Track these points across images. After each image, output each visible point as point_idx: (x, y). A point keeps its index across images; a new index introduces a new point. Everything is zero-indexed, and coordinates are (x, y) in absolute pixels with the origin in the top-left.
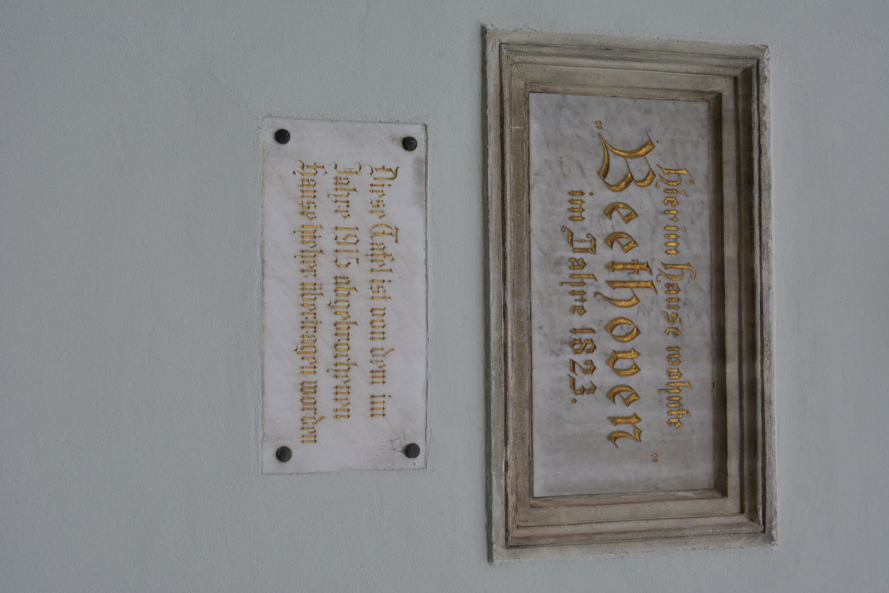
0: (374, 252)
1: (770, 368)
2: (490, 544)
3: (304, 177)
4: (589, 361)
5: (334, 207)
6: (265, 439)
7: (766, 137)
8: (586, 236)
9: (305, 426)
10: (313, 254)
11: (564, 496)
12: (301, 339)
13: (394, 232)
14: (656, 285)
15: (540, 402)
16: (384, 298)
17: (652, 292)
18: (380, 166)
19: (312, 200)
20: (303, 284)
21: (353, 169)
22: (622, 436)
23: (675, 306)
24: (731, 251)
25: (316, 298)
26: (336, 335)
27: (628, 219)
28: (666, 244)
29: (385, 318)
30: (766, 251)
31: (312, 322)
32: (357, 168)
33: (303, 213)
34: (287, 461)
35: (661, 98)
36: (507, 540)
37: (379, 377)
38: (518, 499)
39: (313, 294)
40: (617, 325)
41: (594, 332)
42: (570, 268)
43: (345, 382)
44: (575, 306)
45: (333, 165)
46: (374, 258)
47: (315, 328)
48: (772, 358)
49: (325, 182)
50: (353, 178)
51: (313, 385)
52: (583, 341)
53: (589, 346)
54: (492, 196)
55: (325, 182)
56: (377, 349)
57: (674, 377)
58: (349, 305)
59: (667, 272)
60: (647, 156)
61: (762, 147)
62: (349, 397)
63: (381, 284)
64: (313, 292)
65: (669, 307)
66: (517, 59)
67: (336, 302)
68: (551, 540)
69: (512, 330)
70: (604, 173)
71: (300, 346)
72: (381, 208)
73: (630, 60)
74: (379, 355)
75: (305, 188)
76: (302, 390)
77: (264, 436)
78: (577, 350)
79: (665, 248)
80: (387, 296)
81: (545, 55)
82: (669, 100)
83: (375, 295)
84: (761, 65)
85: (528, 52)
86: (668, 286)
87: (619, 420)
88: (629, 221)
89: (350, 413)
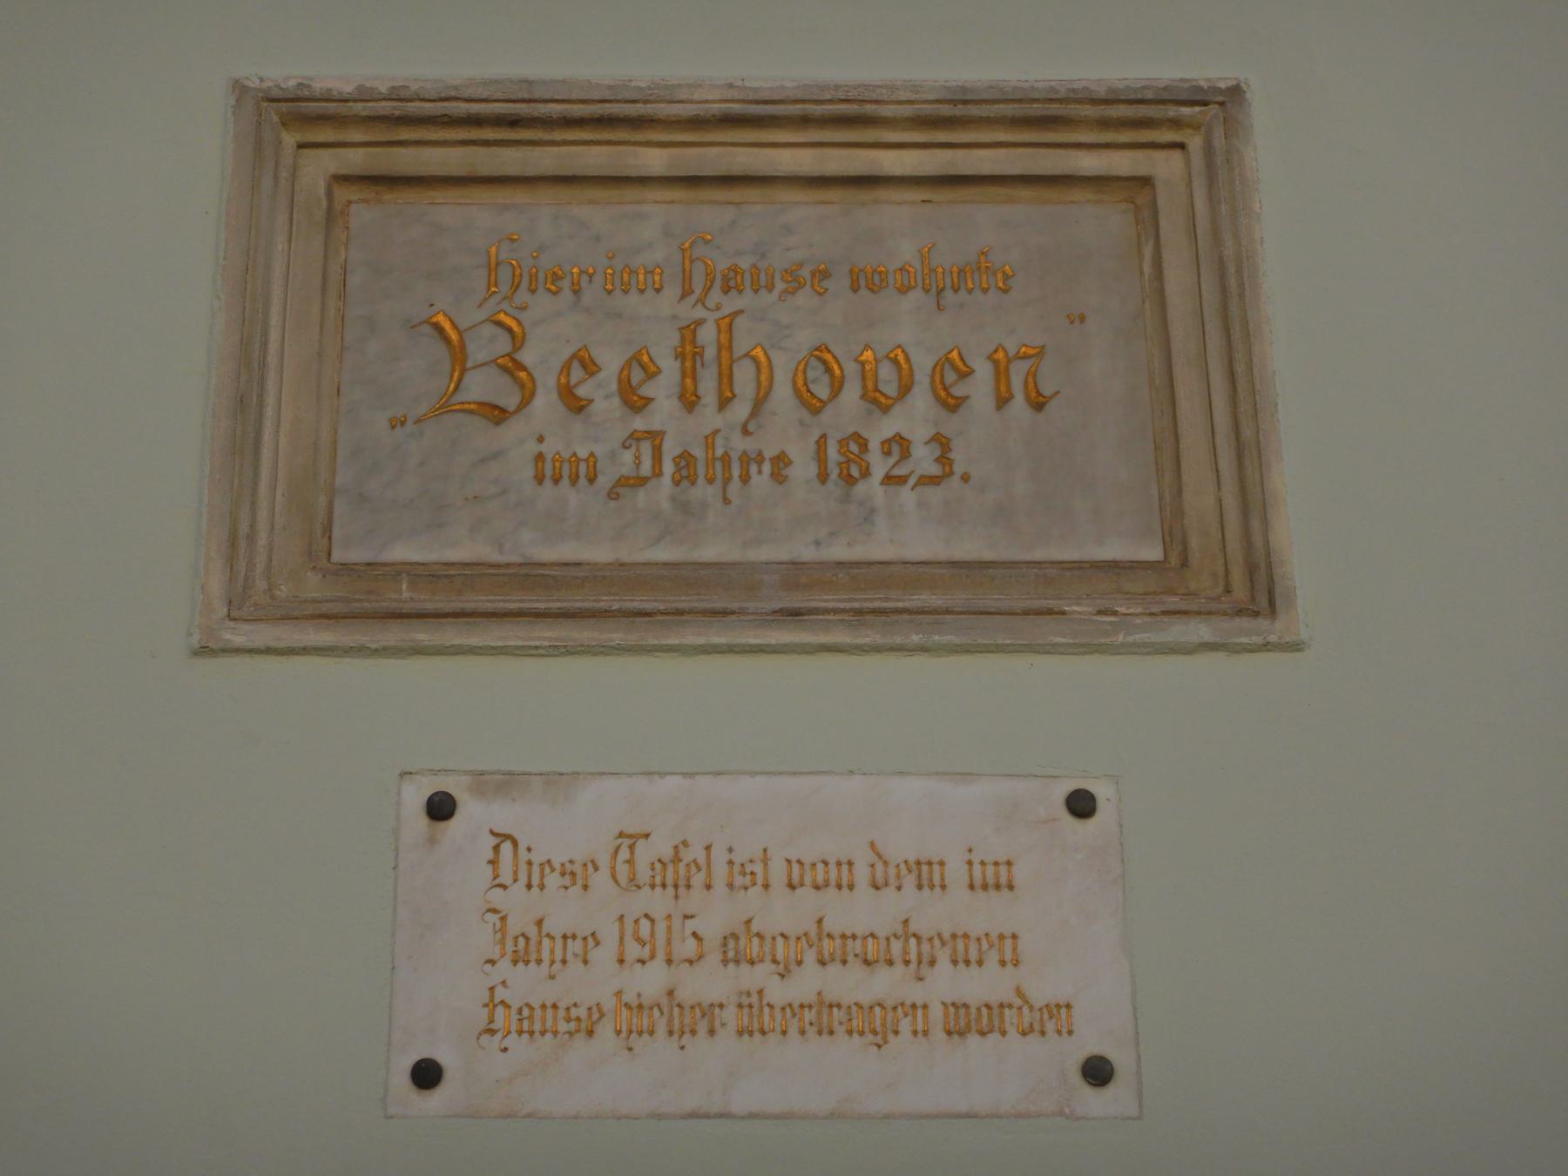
0: (670, 880)
1: (892, 88)
2: (1266, 647)
3: (514, 1028)
4: (883, 448)
5: (575, 967)
6: (1067, 1110)
7: (422, 87)
8: (626, 450)
9: (1037, 1027)
10: (676, 1011)
11: (1161, 498)
12: (855, 1035)
13: (627, 842)
14: (726, 311)
15: (969, 548)
16: (765, 861)
17: (739, 320)
18: (490, 868)
19: (561, 1013)
20: (740, 1033)
21: (494, 924)
22: (1036, 386)
23: (767, 274)
24: (655, 160)
25: (768, 1005)
26: (844, 962)
27: (590, 367)
28: (642, 291)
29: (807, 861)
30: (656, 91)
31: (819, 1012)
32: (489, 916)
33: (590, 1033)
34: (1112, 1065)
35: (340, 296)
36: (1256, 614)
37: (931, 872)
38: (1170, 591)
39: (761, 1010)
40: (809, 391)
41: (824, 436)
42: (693, 483)
43: (943, 944)
44: (772, 474)
45: (488, 967)
46: (681, 883)
47: (831, 1006)
48: (872, 83)
49: (525, 984)
50: (514, 927)
51: (952, 1010)
52: (843, 459)
53: (854, 448)
54: (550, 639)
55: (525, 984)
56: (873, 876)
57: (912, 280)
58: (783, 935)
59: (698, 290)
60: (463, 325)
61: (443, 95)
62: (973, 935)
63: (737, 869)
64: (755, 1011)
65: (770, 288)
66: (262, 585)
67: (775, 961)
68: (1256, 525)
69: (826, 601)
70: (497, 414)
71: (870, 1037)
72: (578, 868)
73: (265, 357)
74: (886, 872)
75: (537, 1027)
76: (961, 1034)
77: (1061, 1113)
78: (860, 470)
79: (650, 293)
80: (760, 854)
81: (253, 526)
82: (345, 280)
83: (760, 881)
84: (275, 93)
85: (248, 563)
86: (726, 290)
87: (1003, 389)
88: (594, 364)
89: (1008, 932)
